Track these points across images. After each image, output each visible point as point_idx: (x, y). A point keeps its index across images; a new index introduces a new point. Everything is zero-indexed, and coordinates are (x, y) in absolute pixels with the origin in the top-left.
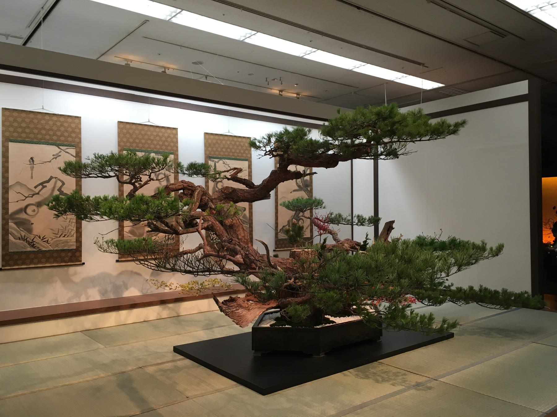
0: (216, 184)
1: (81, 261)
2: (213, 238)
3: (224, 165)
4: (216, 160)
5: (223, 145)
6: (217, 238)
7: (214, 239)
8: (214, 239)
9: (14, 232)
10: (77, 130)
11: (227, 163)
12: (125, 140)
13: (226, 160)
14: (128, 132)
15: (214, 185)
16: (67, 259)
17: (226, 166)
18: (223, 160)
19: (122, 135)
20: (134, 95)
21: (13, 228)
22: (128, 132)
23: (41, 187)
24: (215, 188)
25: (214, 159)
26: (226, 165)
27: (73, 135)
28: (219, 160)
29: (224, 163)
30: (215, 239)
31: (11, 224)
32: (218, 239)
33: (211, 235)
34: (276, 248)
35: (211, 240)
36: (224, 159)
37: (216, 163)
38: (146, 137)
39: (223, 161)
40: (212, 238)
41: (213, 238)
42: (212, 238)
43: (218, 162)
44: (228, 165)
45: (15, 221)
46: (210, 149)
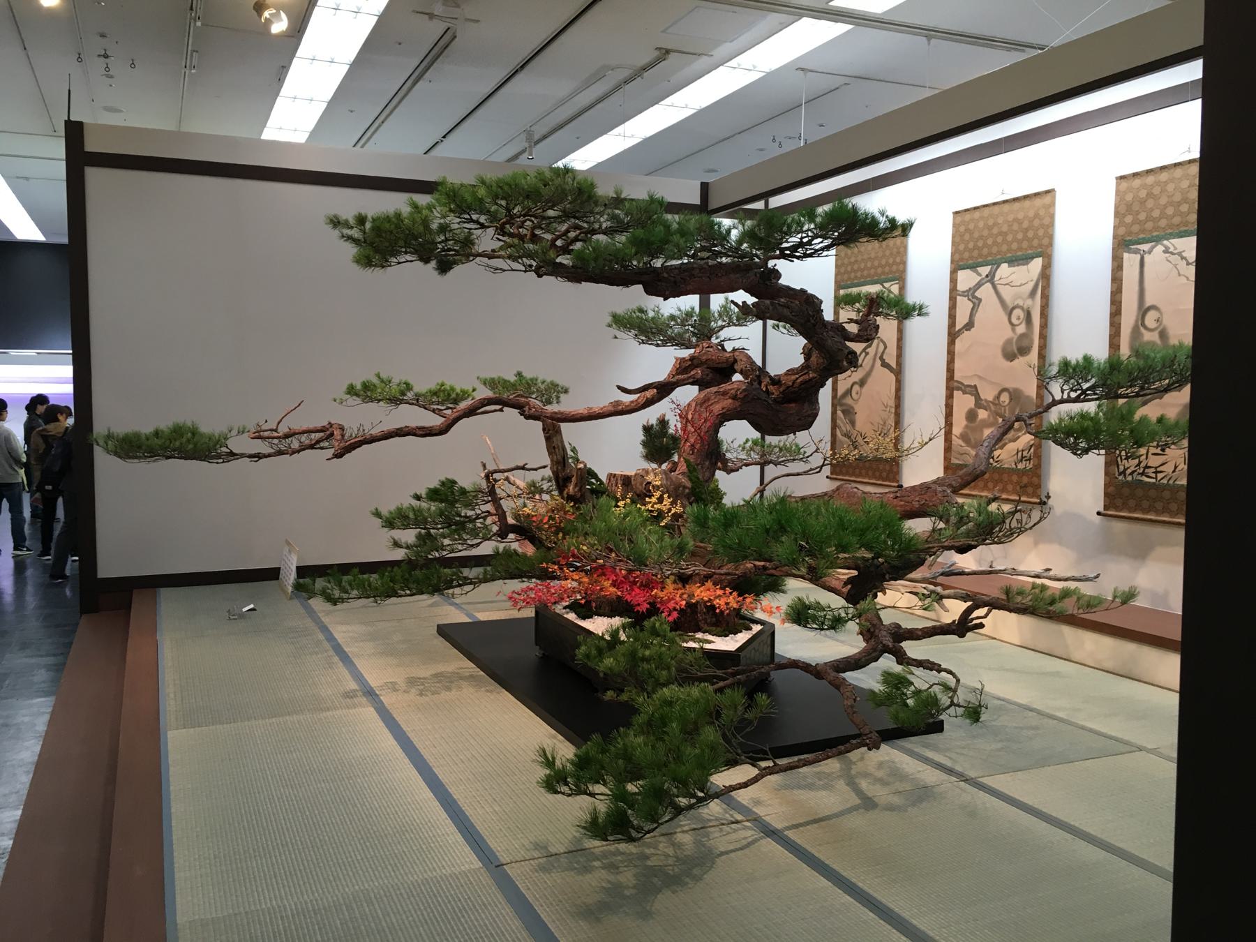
0: (1140, 317)
1: (898, 481)
2: (1125, 470)
3: (1167, 255)
4: (1146, 247)
5: (1168, 197)
6: (1135, 471)
7: (1129, 471)
8: (1129, 471)
9: (842, 425)
10: (902, 249)
11: (1176, 249)
12: (962, 247)
13: (1172, 241)
14: (967, 230)
15: (1137, 321)
16: (884, 474)
17: (1172, 258)
18: (1165, 242)
19: (958, 239)
20: (981, 144)
21: (841, 419)
22: (967, 230)
23: (864, 354)
24: (1139, 329)
25: (1139, 247)
26: (1173, 254)
27: (898, 260)
28: (1153, 244)
29: (1166, 251)
30: (1132, 474)
31: (839, 413)
32: (1139, 474)
33: (1119, 459)
34: (1106, 507)
35: (1120, 474)
36: (1167, 239)
37: (1146, 256)
38: (995, 231)
39: (1163, 245)
40: (1122, 468)
41: (1125, 470)
42: (1122, 468)
43: (1150, 252)
44: (1180, 254)
45: (844, 408)
46: (1129, 219)
